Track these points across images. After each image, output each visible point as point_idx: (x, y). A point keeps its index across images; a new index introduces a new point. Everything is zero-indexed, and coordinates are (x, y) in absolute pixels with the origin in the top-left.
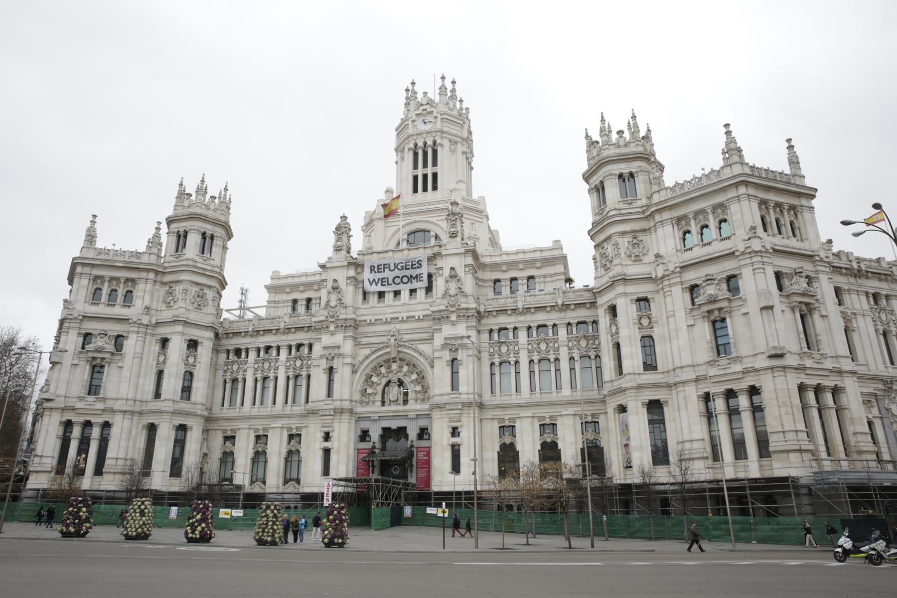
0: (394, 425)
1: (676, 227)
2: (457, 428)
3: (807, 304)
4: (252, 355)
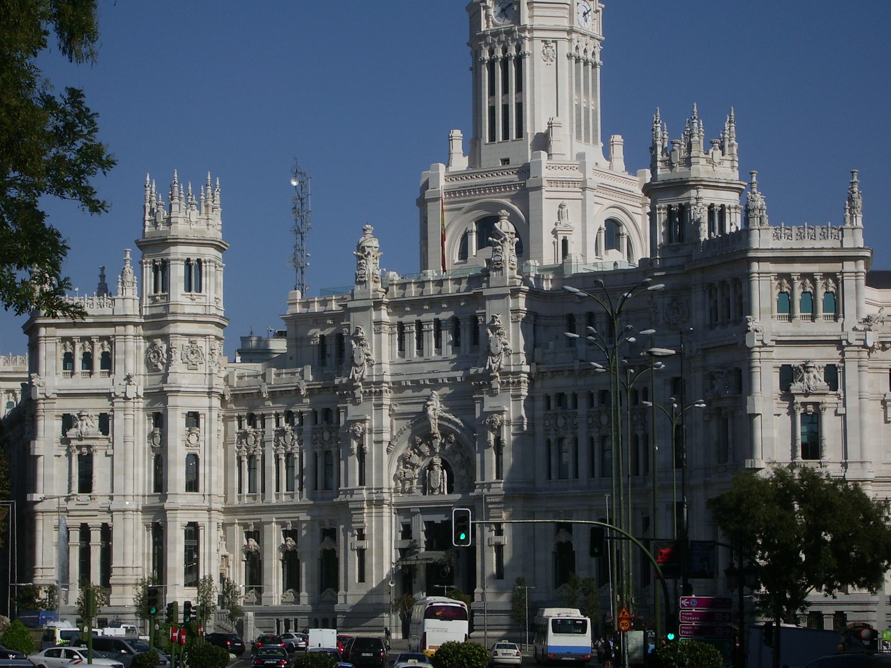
0: (438, 518)
1: (707, 295)
3: (816, 404)
4: (271, 424)
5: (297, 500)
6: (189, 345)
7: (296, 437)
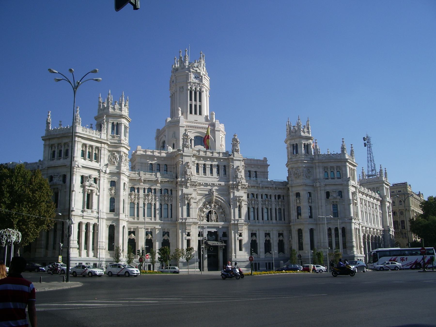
0: (213, 230)
2: (242, 233)
4: (141, 192)
5: (153, 220)
6: (125, 157)
7: (153, 197)
